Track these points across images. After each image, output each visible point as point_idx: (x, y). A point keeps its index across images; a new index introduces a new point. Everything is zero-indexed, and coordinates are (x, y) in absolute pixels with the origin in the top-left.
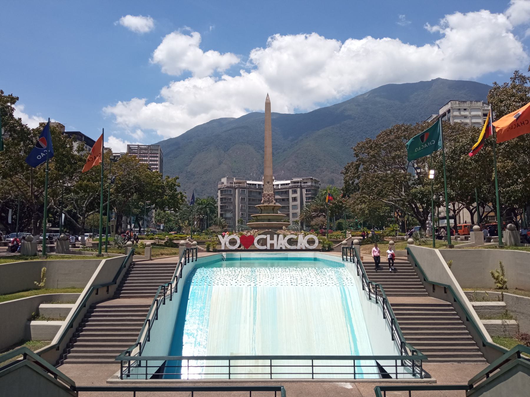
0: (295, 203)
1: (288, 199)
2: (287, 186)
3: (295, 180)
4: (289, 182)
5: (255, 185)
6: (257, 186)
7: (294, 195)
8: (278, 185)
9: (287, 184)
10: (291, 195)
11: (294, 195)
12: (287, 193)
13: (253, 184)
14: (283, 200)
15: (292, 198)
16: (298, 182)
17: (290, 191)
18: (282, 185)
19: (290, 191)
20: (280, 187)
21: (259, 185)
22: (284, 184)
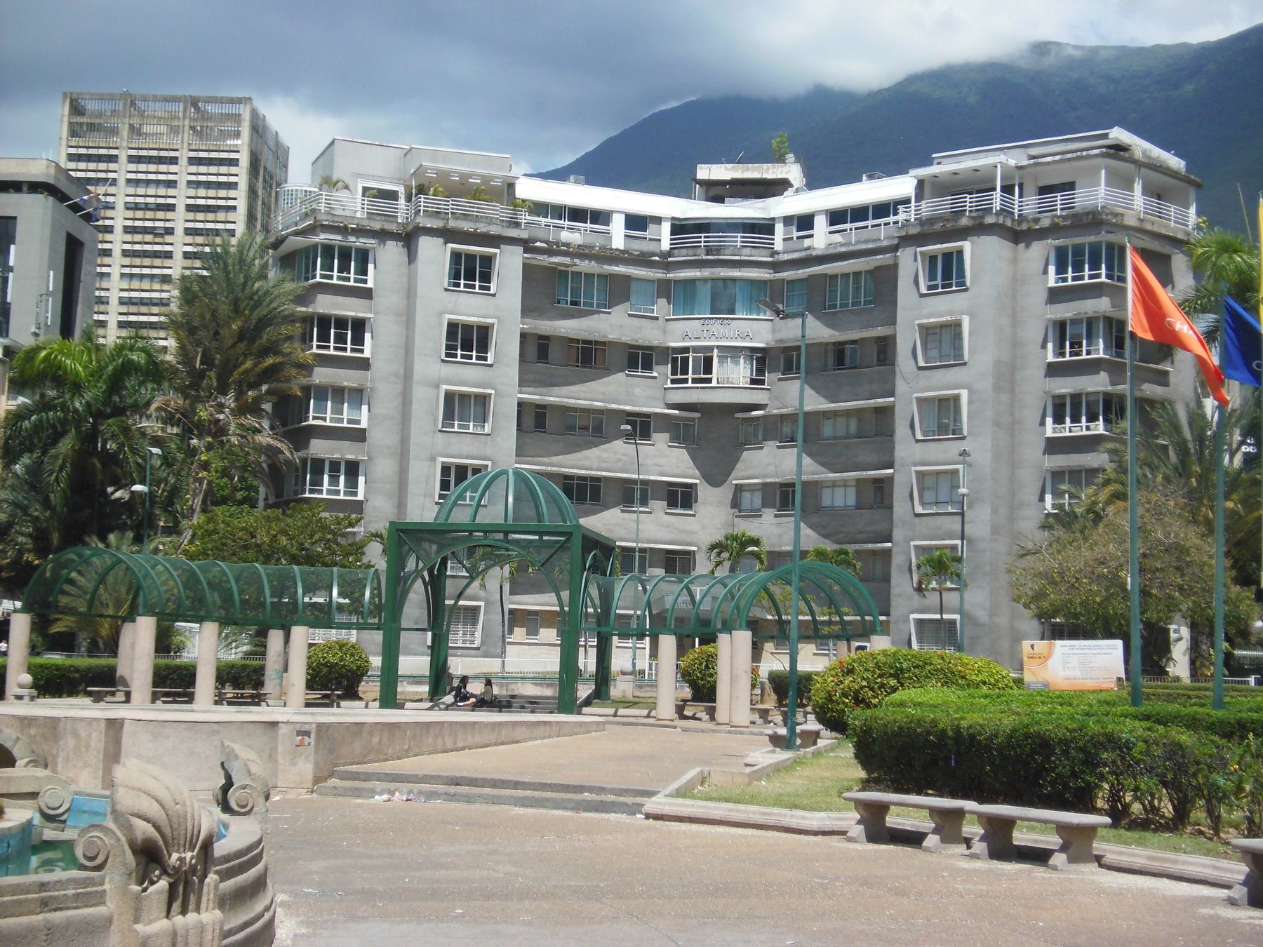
0: (941, 383)
1: (884, 350)
2: (882, 231)
3: (946, 165)
4: (901, 186)
5: (600, 217)
6: (618, 223)
7: (942, 308)
8: (805, 222)
9: (883, 209)
10: (916, 308)
11: (942, 308)
12: (881, 285)
13: (577, 214)
14: (839, 355)
15: (928, 332)
16: (980, 184)
17: (910, 263)
18: (837, 217)
19: (910, 263)
20: (821, 238)
21: (636, 222)
22: (859, 213)
